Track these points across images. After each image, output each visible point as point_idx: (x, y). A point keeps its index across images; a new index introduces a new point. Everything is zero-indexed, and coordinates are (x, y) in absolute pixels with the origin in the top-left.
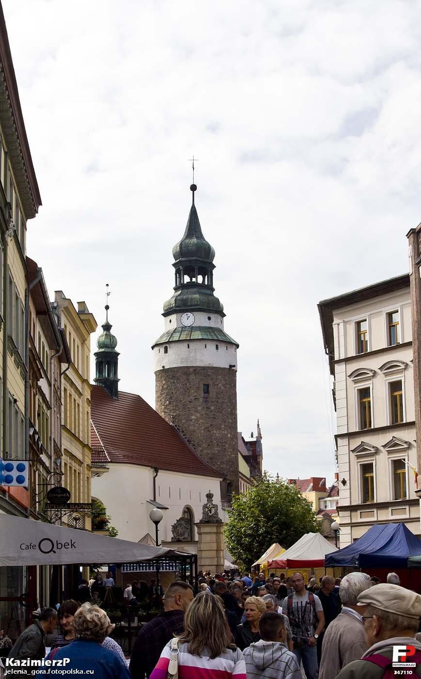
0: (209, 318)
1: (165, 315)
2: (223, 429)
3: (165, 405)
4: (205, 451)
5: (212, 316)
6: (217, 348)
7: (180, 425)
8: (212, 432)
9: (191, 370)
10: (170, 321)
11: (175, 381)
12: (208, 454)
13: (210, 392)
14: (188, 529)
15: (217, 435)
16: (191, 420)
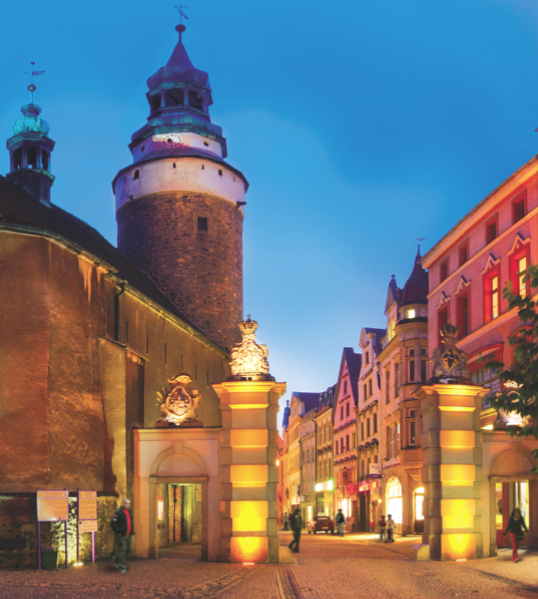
6: (220, 173)
13: (209, 228)
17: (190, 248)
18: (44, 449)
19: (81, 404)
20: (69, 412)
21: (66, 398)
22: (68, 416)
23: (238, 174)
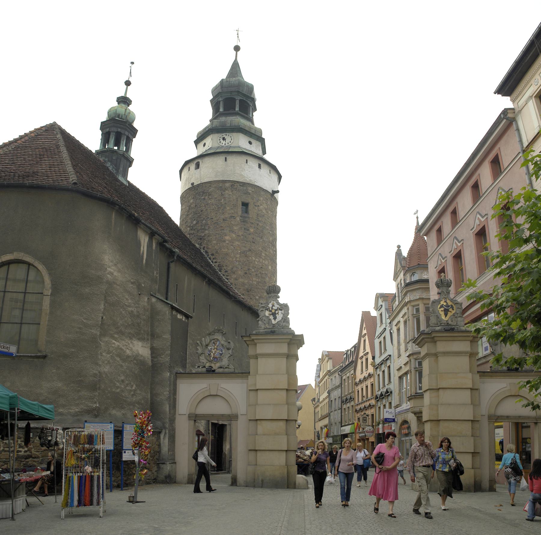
0: (250, 143)
1: (197, 142)
2: (263, 258)
3: (192, 225)
4: (241, 280)
5: (252, 140)
6: (260, 166)
7: (210, 247)
8: (251, 258)
9: (227, 185)
10: (204, 145)
11: (206, 197)
12: (243, 284)
13: (250, 212)
14: (228, 349)
15: (256, 263)
16: (224, 241)
17: (235, 228)
18: (94, 387)
19: (131, 350)
20: (119, 355)
21: (117, 343)
22: (118, 359)
23: (274, 168)
